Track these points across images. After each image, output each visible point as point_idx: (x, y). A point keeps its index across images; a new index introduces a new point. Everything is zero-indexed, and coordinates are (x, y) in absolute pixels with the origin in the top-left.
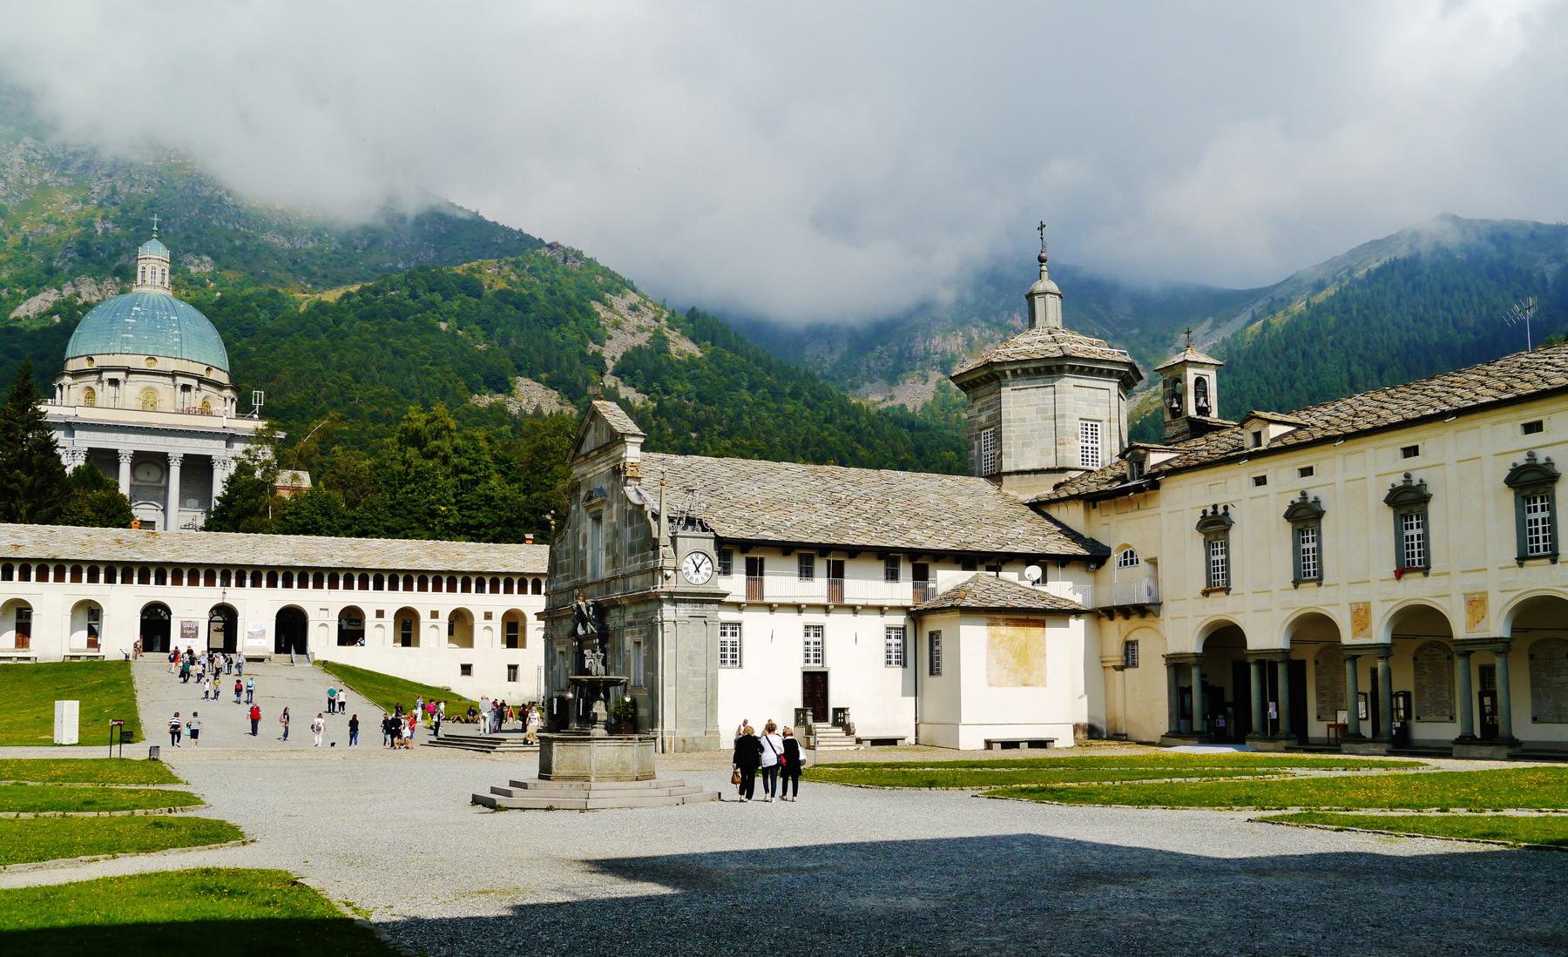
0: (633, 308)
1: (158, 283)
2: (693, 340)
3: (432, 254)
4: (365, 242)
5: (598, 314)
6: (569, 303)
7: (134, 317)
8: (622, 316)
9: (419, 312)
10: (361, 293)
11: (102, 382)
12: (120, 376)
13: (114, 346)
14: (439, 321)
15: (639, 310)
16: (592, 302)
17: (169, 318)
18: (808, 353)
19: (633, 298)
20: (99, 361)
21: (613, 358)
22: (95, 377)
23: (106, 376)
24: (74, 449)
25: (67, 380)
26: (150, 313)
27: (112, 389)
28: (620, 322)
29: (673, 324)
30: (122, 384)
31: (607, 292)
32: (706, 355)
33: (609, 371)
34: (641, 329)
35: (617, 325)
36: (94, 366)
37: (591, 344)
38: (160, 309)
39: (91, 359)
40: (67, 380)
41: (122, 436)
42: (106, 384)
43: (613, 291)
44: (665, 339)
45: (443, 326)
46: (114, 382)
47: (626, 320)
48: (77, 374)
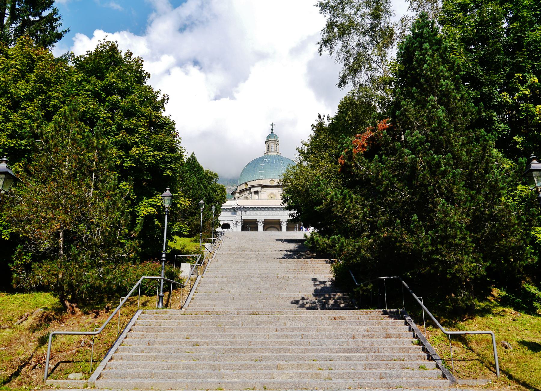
1: (274, 150)
7: (264, 163)
11: (251, 193)
12: (258, 189)
13: (256, 177)
17: (279, 162)
20: (250, 184)
22: (248, 192)
23: (253, 190)
24: (236, 220)
25: (237, 195)
26: (271, 161)
27: (256, 196)
30: (259, 193)
36: (248, 187)
38: (275, 159)
39: (246, 184)
40: (237, 195)
41: (258, 213)
42: (253, 194)
46: (256, 192)
48: (241, 192)
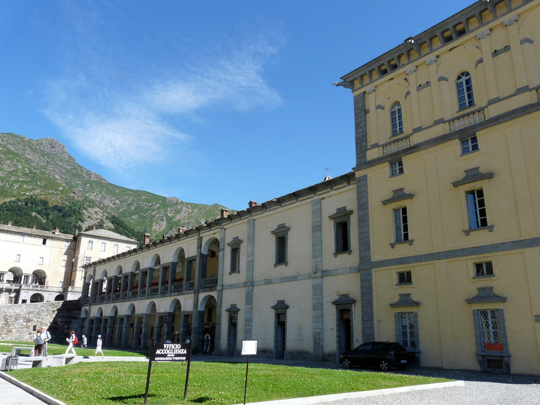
0: (96, 212)
2: (112, 223)
3: (38, 191)
4: (18, 186)
5: (84, 214)
6: (75, 210)
8: (92, 215)
9: (26, 209)
10: (10, 202)
14: (33, 212)
15: (98, 213)
16: (83, 210)
18: (153, 228)
19: (97, 209)
21: (85, 227)
28: (90, 216)
29: (107, 218)
31: (89, 207)
32: (115, 228)
33: (83, 230)
34: (97, 219)
35: (89, 217)
37: (80, 222)
43: (91, 207)
44: (104, 223)
45: (34, 214)
47: (93, 216)
